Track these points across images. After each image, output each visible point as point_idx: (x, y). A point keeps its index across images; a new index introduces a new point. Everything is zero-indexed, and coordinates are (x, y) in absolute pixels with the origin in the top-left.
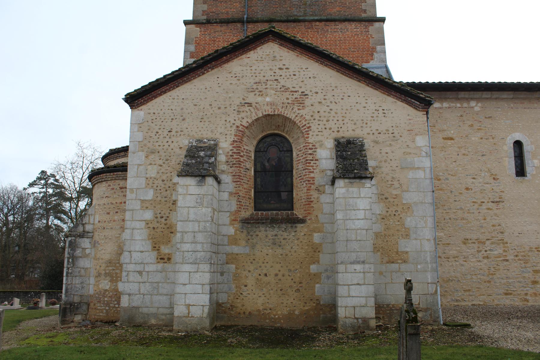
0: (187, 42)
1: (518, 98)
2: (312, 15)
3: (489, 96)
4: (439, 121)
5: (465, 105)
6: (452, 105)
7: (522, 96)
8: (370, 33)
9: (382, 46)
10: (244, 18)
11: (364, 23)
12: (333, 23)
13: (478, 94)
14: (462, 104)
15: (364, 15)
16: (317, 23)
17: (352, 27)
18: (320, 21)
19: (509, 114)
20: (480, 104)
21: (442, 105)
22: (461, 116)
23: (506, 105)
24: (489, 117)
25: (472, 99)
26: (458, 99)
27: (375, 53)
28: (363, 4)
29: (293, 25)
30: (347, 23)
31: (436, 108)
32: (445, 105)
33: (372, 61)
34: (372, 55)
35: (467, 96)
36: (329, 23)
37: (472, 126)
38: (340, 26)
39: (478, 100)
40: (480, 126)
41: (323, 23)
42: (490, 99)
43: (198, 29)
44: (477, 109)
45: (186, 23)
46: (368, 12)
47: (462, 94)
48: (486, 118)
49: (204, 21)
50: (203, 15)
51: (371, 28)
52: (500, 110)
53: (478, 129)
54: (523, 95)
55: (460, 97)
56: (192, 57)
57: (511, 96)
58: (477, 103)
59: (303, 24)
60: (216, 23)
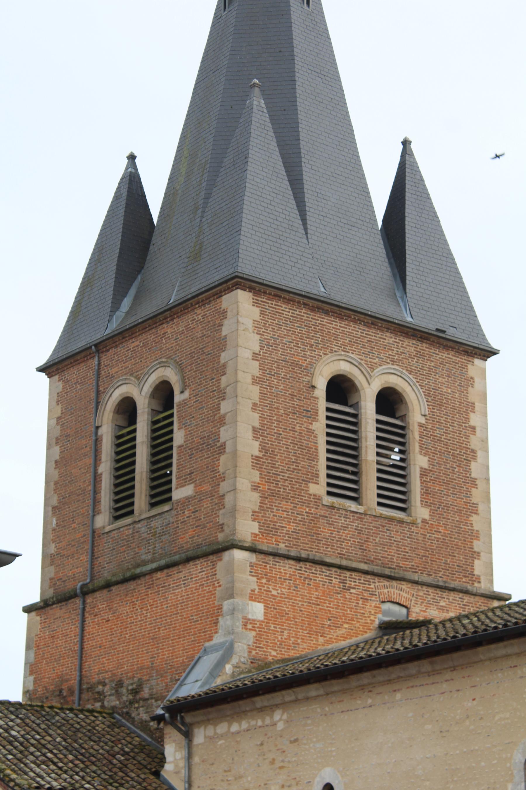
0: (28, 647)
1: (333, 692)
2: (152, 561)
3: (293, 698)
4: (236, 758)
5: (268, 721)
6: (253, 723)
7: (335, 688)
8: (218, 576)
9: (231, 601)
10: (76, 589)
11: (211, 557)
12: (175, 569)
13: (277, 697)
14: (272, 717)
15: (221, 537)
16: (159, 575)
17: (197, 570)
18: (160, 569)
19: (321, 728)
20: (285, 716)
21: (240, 726)
22: (262, 744)
23: (319, 710)
24: (296, 740)
25: (277, 706)
26: (262, 710)
27: (220, 618)
28: (221, 512)
29: (132, 585)
30: (191, 563)
31: (233, 733)
32: (244, 725)
33: (216, 635)
34: (216, 623)
35: (266, 704)
36: (171, 569)
37: (273, 762)
38: (185, 571)
39: (283, 705)
40: (283, 761)
41: (165, 571)
42: (296, 701)
43: (38, 618)
44: (280, 726)
45: (28, 610)
46: (225, 528)
47: (260, 701)
48: (291, 742)
49: (42, 604)
50: (50, 587)
51: (220, 566)
52: (309, 722)
53: (281, 768)
54: (336, 685)
55: (259, 705)
56: (31, 673)
57: (321, 692)
58: (283, 713)
59: (142, 580)
60: (54, 603)
